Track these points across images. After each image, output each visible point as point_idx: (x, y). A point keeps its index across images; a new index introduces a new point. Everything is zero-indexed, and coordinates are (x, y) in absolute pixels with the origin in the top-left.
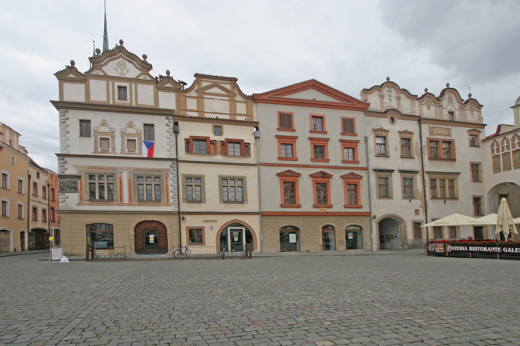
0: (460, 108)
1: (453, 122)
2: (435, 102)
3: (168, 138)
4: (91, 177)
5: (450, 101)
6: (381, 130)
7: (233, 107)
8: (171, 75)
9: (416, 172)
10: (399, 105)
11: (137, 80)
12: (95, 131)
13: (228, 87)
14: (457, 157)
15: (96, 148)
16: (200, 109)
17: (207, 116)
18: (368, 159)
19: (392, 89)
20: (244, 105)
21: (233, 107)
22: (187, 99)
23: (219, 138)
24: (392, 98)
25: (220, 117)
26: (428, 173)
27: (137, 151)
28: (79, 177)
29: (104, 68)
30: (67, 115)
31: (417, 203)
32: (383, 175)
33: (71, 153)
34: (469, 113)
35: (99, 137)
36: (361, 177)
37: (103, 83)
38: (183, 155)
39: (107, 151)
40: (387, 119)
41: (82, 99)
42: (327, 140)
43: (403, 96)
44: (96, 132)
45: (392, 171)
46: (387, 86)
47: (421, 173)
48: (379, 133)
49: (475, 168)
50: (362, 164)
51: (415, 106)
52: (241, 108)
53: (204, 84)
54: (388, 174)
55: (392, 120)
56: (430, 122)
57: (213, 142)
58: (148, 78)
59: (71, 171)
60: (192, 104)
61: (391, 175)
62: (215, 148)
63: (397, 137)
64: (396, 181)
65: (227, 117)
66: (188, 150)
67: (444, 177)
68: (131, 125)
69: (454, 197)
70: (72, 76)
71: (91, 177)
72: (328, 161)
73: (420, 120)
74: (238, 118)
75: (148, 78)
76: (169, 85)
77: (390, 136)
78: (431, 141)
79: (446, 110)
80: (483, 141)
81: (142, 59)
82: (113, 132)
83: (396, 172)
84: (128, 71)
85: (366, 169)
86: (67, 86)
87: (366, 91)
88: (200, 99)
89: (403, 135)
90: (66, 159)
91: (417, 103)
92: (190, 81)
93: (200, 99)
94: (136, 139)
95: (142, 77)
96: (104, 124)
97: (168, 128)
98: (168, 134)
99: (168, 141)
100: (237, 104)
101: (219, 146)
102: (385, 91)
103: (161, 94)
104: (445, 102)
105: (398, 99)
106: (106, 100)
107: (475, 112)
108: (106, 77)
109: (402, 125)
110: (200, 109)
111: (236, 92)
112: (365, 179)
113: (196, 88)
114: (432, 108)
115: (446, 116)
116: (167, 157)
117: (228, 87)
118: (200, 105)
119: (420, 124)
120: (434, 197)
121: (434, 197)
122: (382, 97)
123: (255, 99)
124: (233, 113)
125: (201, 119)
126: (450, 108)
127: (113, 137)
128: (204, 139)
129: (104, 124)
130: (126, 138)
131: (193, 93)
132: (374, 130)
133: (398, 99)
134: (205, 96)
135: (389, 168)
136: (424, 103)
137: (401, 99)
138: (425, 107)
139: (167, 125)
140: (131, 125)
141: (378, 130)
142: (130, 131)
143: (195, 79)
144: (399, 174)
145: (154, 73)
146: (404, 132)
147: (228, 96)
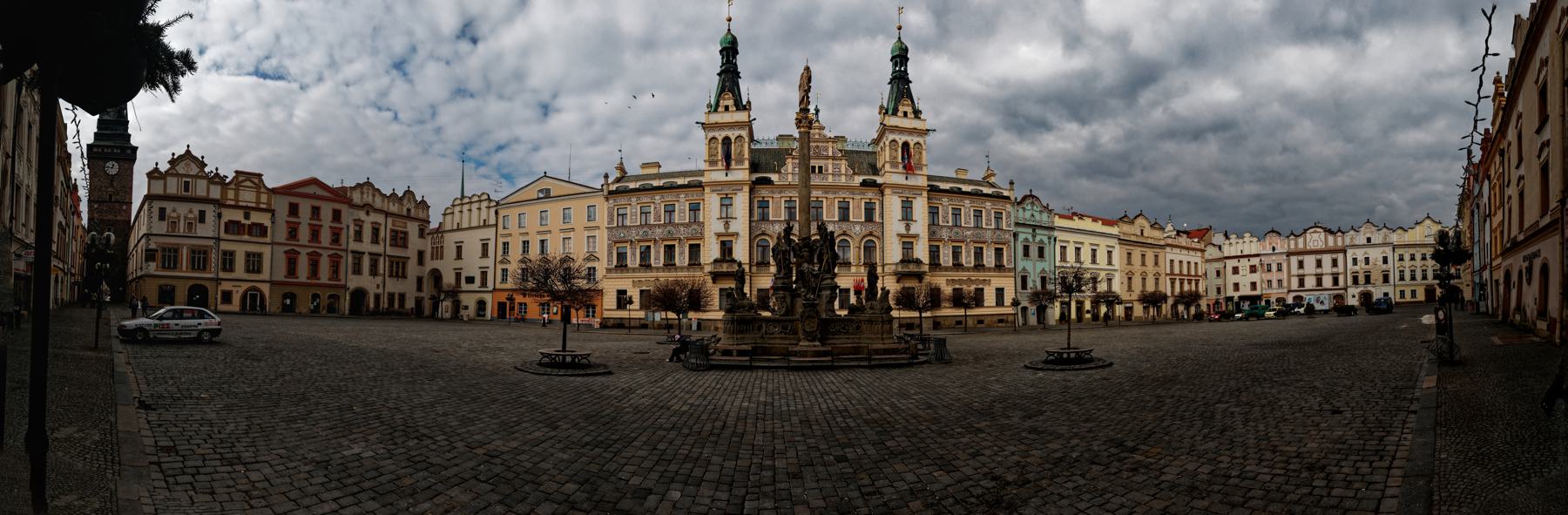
5: (409, 201)
14: (410, 246)
31: (379, 280)
32: (357, 255)
42: (321, 226)
49: (421, 254)
50: (344, 247)
64: (366, 261)
69: (404, 276)
72: (320, 242)
78: (392, 231)
80: (428, 234)
85: (346, 250)
104: (405, 202)
112: (345, 258)
114: (396, 204)
115: (405, 213)
119: (386, 217)
120: (391, 276)
121: (391, 276)
138: (391, 204)
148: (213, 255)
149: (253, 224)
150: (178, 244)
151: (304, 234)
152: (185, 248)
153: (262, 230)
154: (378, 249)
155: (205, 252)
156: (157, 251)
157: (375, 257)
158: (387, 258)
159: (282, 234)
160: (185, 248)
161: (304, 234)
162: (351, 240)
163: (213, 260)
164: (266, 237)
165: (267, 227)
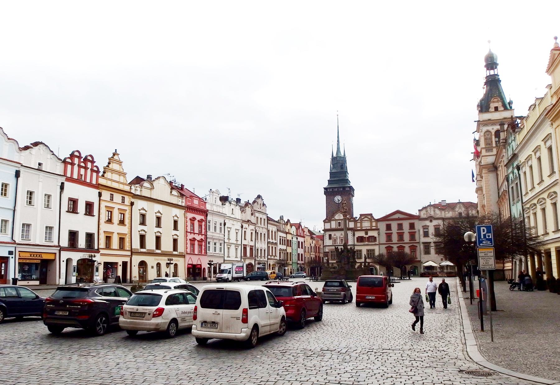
2: (451, 210)
3: (352, 238)
4: (332, 252)
7: (371, 224)
13: (370, 217)
15: (333, 243)
16: (361, 227)
17: (363, 228)
18: (420, 239)
19: (432, 207)
20: (375, 223)
21: (371, 224)
22: (357, 223)
23: (367, 236)
24: (431, 211)
25: (367, 228)
28: (329, 252)
29: (335, 217)
32: (426, 244)
33: (327, 245)
36: (417, 246)
38: (356, 243)
39: (336, 244)
40: (428, 221)
41: (329, 228)
42: (404, 233)
43: (436, 210)
45: (430, 243)
48: (425, 227)
50: (417, 241)
51: (442, 213)
52: (374, 224)
53: (362, 217)
54: (429, 244)
55: (431, 221)
59: (327, 251)
60: (359, 225)
61: (430, 244)
62: (366, 239)
65: (369, 228)
66: (357, 241)
70: (327, 221)
71: (332, 252)
74: (373, 228)
76: (352, 220)
77: (429, 228)
82: (337, 237)
85: (419, 243)
86: (325, 224)
91: (443, 212)
92: (358, 217)
93: (361, 223)
96: (335, 235)
97: (352, 234)
98: (352, 236)
102: (428, 209)
103: (350, 223)
108: (336, 220)
109: (435, 222)
113: (360, 219)
116: (351, 244)
117: (370, 217)
118: (361, 225)
122: (427, 211)
123: (378, 220)
124: (371, 226)
126: (460, 211)
131: (359, 221)
132: (423, 226)
133: (434, 211)
134: (363, 222)
136: (446, 211)
140: (342, 235)
141: (424, 226)
142: (342, 236)
151: (395, 238)
153: (373, 239)
159: (383, 239)
161: (395, 238)
162: (422, 237)
164: (376, 242)
165: (376, 237)
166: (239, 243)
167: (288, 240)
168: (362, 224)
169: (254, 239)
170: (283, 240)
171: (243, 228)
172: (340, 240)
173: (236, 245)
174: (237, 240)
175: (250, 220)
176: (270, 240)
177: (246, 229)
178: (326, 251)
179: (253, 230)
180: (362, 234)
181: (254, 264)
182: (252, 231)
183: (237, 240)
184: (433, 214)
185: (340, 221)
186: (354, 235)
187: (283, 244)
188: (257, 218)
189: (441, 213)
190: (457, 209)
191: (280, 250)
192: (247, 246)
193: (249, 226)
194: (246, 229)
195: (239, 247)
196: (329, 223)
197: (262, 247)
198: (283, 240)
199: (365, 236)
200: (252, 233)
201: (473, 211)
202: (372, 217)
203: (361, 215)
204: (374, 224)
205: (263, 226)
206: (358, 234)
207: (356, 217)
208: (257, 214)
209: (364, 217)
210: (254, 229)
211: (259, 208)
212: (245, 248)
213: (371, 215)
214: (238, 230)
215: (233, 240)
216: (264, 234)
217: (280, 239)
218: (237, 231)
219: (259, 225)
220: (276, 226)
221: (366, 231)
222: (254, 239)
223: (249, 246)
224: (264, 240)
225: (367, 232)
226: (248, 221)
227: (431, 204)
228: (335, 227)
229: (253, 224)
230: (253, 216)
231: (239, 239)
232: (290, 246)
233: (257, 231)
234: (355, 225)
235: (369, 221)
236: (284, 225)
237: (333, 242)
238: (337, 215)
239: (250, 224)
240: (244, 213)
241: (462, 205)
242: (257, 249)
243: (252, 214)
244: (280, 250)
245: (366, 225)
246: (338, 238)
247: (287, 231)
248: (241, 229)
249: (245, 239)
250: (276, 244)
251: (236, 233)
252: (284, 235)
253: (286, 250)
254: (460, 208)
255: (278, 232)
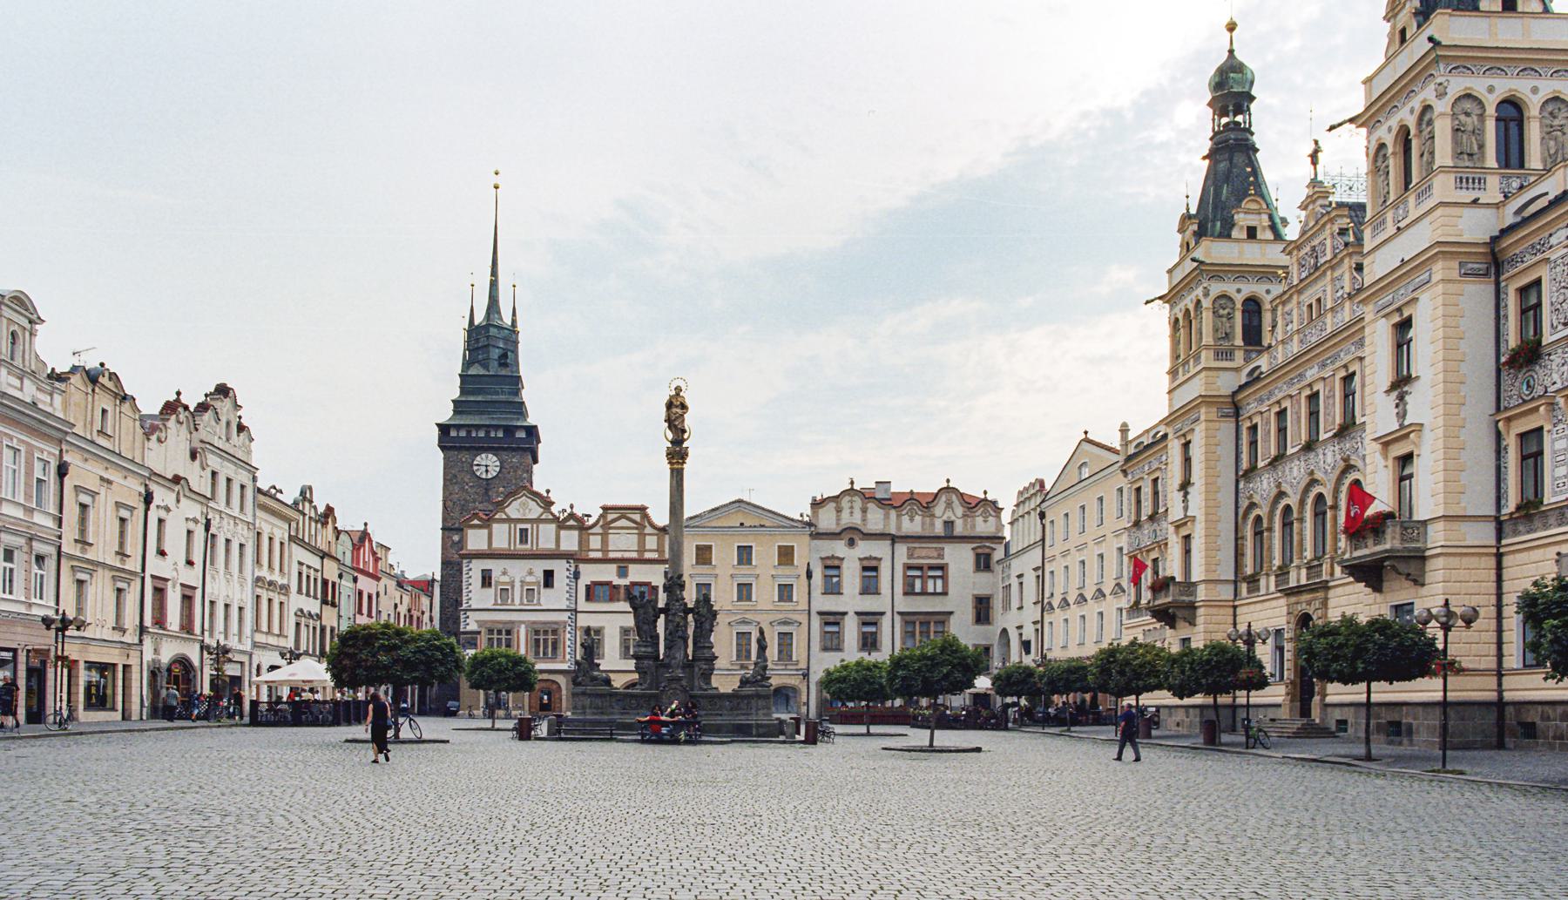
0: (964, 516)
1: (950, 537)
6: (833, 557)
7: (642, 543)
8: (575, 511)
9: (882, 614)
10: (864, 519)
11: (539, 521)
12: (496, 582)
15: (496, 600)
16: (604, 549)
17: (612, 555)
19: (856, 498)
21: (642, 543)
22: (591, 537)
25: (627, 555)
26: (899, 613)
27: (535, 602)
30: (471, 566)
33: (473, 607)
34: (979, 520)
35: (500, 587)
37: (506, 526)
38: (583, 605)
41: (484, 547)
43: (871, 506)
44: (496, 582)
46: (849, 495)
47: (889, 614)
48: (829, 563)
52: (651, 542)
53: (610, 517)
55: (851, 543)
56: (909, 540)
57: (616, 587)
58: (551, 517)
60: (595, 542)
61: (843, 619)
63: (857, 566)
65: (634, 555)
66: (589, 598)
67: (928, 618)
68: (530, 573)
70: (476, 522)
73: (894, 539)
74: (648, 555)
75: (551, 517)
76: (572, 522)
77: (845, 565)
79: (940, 520)
81: (545, 494)
82: (513, 582)
83: (851, 614)
84: (530, 510)
87: (817, 504)
88: (605, 536)
89: (866, 563)
90: (468, 613)
91: (893, 513)
92: (596, 513)
93: (605, 536)
94: (535, 588)
95: (543, 517)
96: (504, 573)
97: (567, 573)
99: (568, 588)
100: (647, 537)
101: (622, 591)
103: (563, 533)
105: (864, 511)
106: (506, 546)
107: (990, 519)
108: (509, 520)
109: (865, 549)
110: (604, 549)
111: (647, 524)
113: (601, 523)
116: (565, 608)
117: (637, 517)
118: (605, 542)
122: (839, 510)
124: (642, 549)
125: (605, 561)
127: (513, 587)
128: (608, 584)
129: (504, 573)
130: (526, 587)
131: (597, 529)
132: (822, 559)
133: (864, 511)
134: (611, 531)
135: (842, 609)
136: (904, 512)
137: (869, 511)
139: (568, 570)
140: (530, 573)
141: (828, 558)
142: (529, 579)
143: (601, 511)
144: (856, 617)
145: (555, 509)
146: (866, 558)
147: (636, 528)
148: (568, 636)
149: (634, 584)
150: (512, 622)
152: (523, 626)
154: (870, 604)
155: (555, 632)
156: (479, 633)
157: (869, 619)
158: (898, 618)
160: (523, 626)
163: (568, 643)
166: (133, 565)
167: (325, 582)
168: (607, 538)
169: (197, 558)
170: (308, 577)
171: (153, 506)
172: (522, 591)
173: (120, 574)
174: (122, 554)
175: (182, 475)
176: (264, 572)
177: (168, 509)
178: (469, 628)
179: (195, 521)
180: (608, 574)
181: (196, 663)
182: (191, 526)
183: (122, 554)
184: (859, 522)
185: (528, 526)
186: (577, 575)
187: (308, 595)
188: (214, 474)
189: (887, 517)
190: (939, 509)
191: (299, 613)
192: (170, 583)
193: (178, 501)
194: (168, 509)
195: (132, 583)
196: (485, 532)
197: (230, 594)
198: (308, 577)
199: (617, 581)
200: (189, 532)
201: (990, 518)
202: (645, 516)
203: (606, 509)
204: (651, 542)
205: (236, 512)
206: (590, 574)
207: (589, 516)
208: (213, 461)
209: (615, 516)
210: (199, 517)
211: (224, 438)
212: (160, 592)
213: (642, 510)
214: (132, 509)
215: (103, 549)
216: (241, 546)
217: (300, 574)
218: (124, 513)
219: (222, 506)
220: (288, 520)
221: (623, 565)
222: (197, 558)
223: (178, 588)
224: (241, 571)
225: (626, 567)
226: (177, 479)
227: (856, 487)
228: (506, 546)
229: (194, 496)
230: (197, 462)
231: (134, 548)
232: (333, 605)
233: (213, 530)
234: (583, 542)
235: (636, 531)
236: (313, 524)
237: (496, 595)
238: (516, 504)
239: (185, 496)
240: (159, 440)
241: (954, 497)
242: (212, 603)
243: (193, 456)
244: (300, 613)
245: (623, 542)
246: (517, 585)
247: (324, 547)
248: (142, 507)
249: (162, 553)
250: (285, 589)
251: (117, 523)
252: (314, 561)
253: (319, 617)
254: (949, 505)
255: (294, 546)
